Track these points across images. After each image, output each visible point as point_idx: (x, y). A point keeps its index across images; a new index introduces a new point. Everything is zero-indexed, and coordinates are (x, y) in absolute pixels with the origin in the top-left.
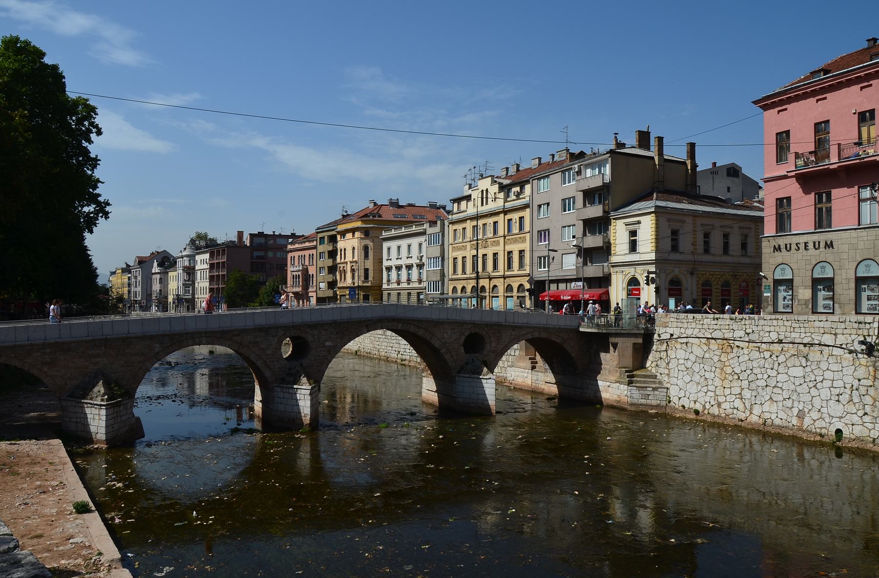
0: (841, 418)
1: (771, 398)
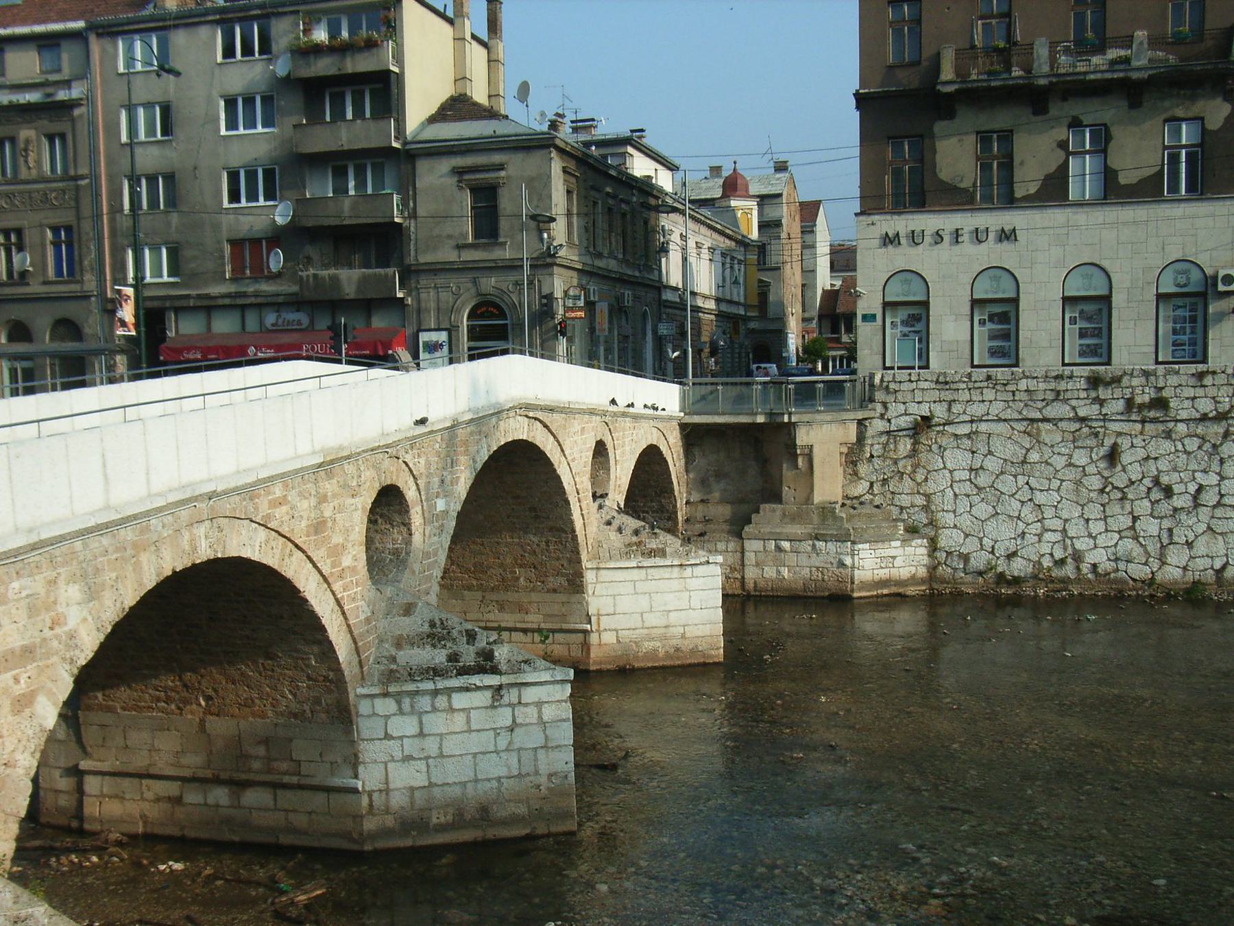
1: (1210, 528)
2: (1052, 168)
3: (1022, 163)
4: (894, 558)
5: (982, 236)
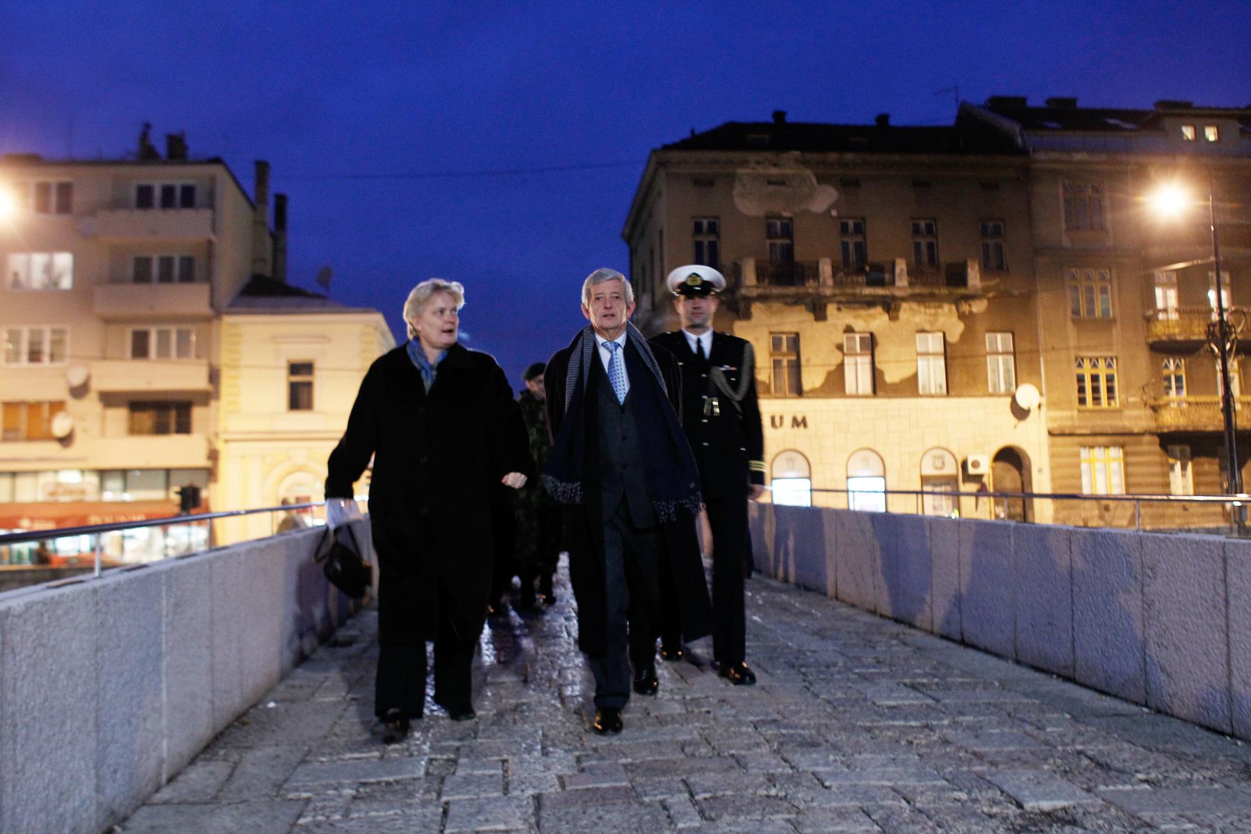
2: (832, 368)
3: (808, 361)
5: (777, 421)
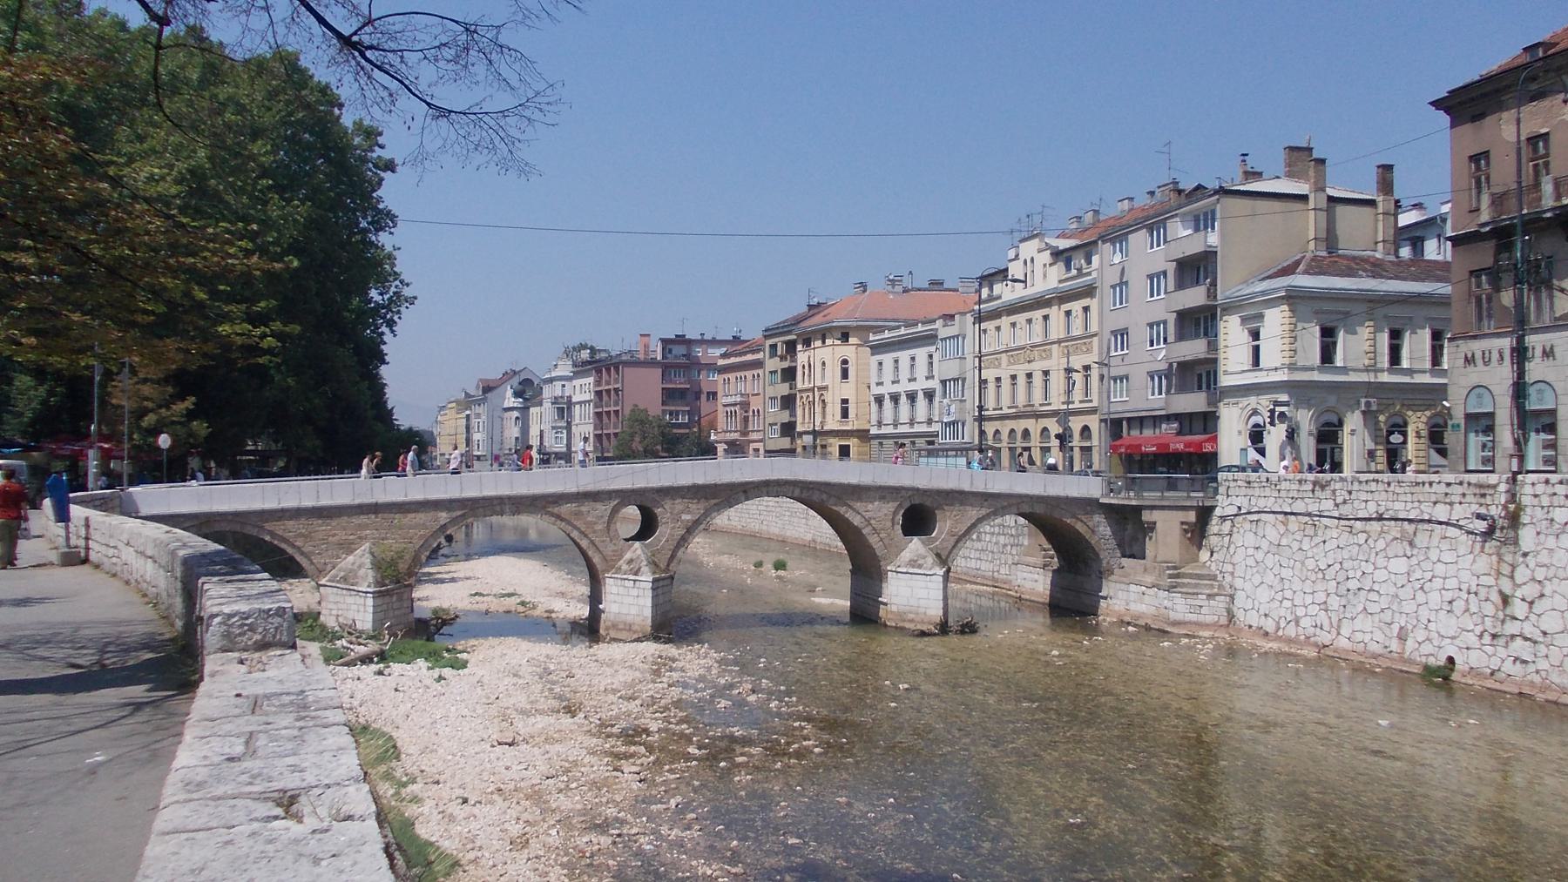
0: (1453, 638)
1: (1365, 609)
4: (1201, 607)
